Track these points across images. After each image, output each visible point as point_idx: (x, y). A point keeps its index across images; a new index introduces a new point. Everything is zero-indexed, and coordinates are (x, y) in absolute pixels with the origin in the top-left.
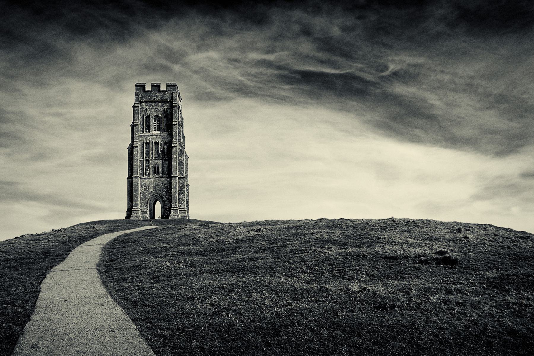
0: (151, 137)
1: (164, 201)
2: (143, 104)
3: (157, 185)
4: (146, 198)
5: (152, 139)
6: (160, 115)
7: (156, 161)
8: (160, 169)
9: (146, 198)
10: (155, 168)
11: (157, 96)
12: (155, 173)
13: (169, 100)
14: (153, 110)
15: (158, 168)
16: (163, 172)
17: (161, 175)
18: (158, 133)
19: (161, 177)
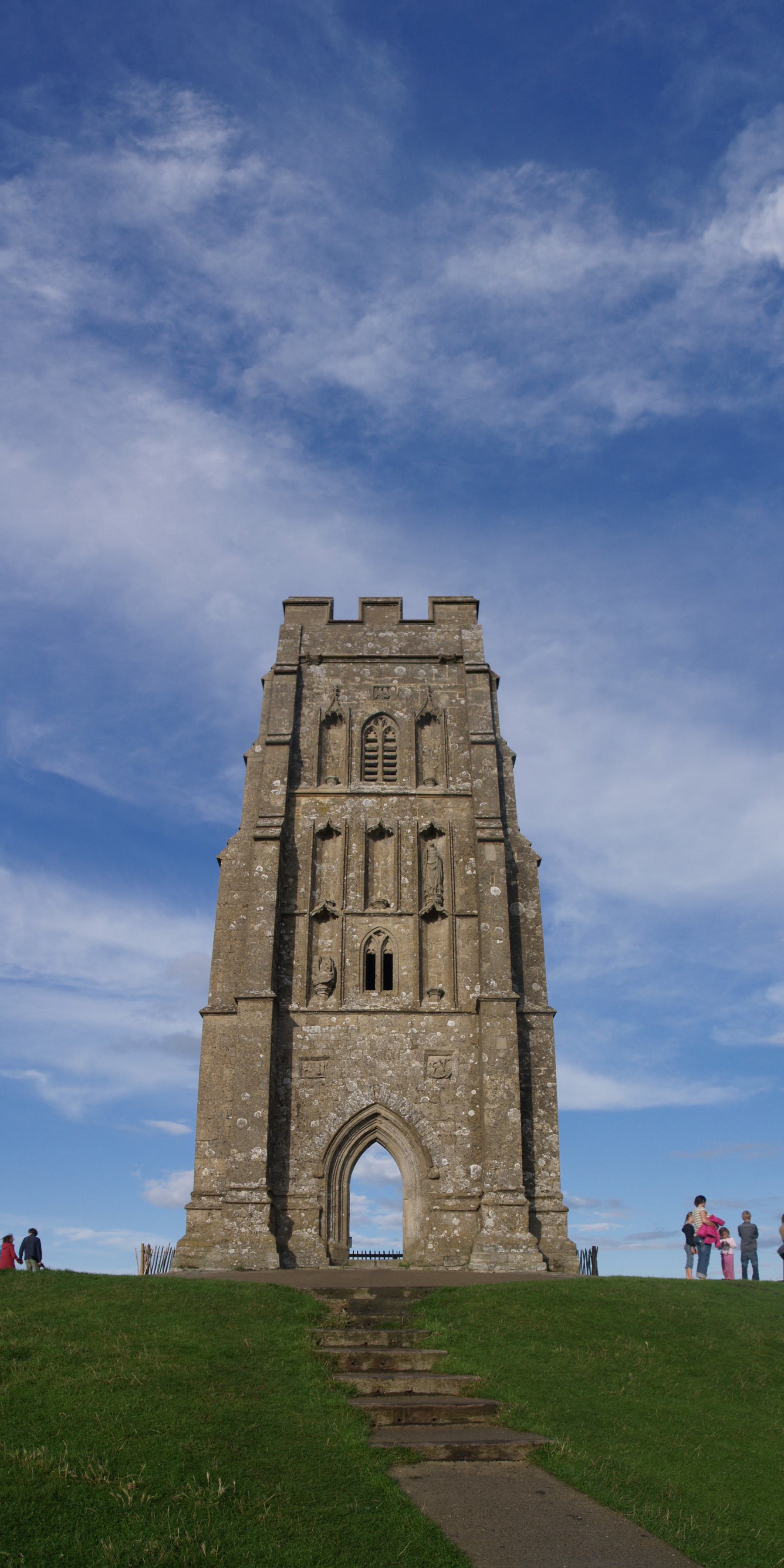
0: (349, 803)
1: (427, 1155)
2: (317, 671)
3: (383, 1055)
4: (312, 1132)
5: (356, 811)
6: (398, 714)
7: (380, 923)
8: (404, 969)
9: (312, 1132)
10: (370, 960)
11: (384, 641)
12: (369, 985)
13: (442, 652)
14: (363, 695)
15: (388, 959)
16: (421, 980)
17: (405, 996)
18: (390, 788)
19: (405, 1012)
